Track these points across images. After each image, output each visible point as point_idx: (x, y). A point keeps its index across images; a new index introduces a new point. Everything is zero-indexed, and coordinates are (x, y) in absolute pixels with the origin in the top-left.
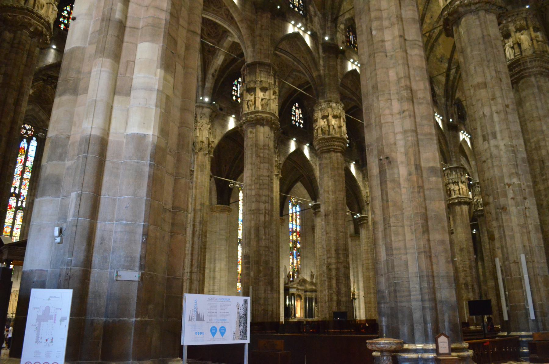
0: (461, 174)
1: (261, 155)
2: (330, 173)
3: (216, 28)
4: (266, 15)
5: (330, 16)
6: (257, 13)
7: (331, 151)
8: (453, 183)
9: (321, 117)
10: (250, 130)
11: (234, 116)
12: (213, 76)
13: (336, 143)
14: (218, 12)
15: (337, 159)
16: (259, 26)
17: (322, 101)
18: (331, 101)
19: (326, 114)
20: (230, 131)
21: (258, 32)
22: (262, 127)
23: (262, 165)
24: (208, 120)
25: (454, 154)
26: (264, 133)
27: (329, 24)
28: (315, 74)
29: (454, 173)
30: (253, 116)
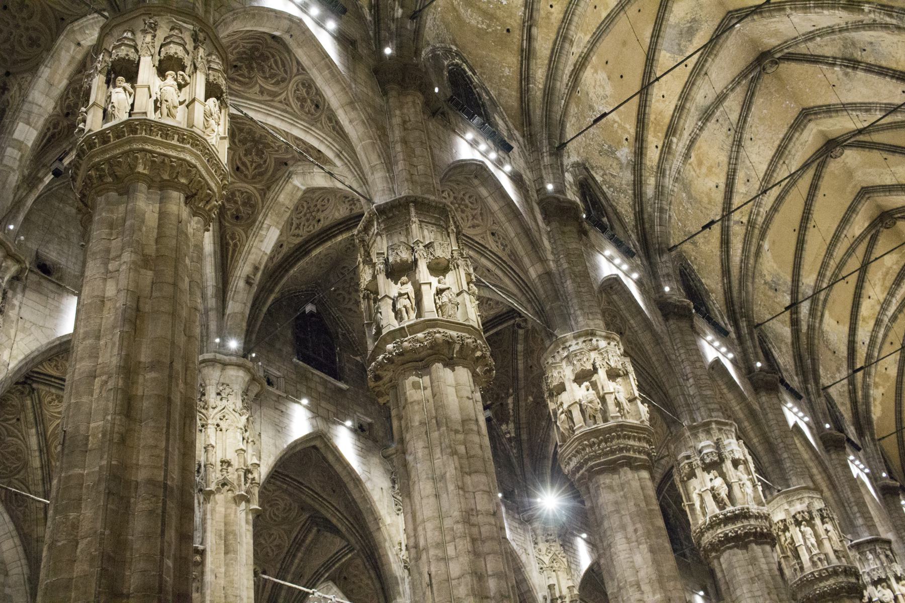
0: (887, 556)
1: (462, 449)
2: (630, 529)
3: (260, 153)
4: (410, 99)
5: (545, 142)
6: (385, 93)
7: (622, 465)
8: (875, 583)
9: (573, 377)
10: (413, 378)
11: (305, 401)
12: (248, 282)
13: (631, 442)
14: (274, 95)
15: (642, 488)
16: (396, 121)
17: (569, 335)
18: (593, 334)
19: (589, 367)
20: (296, 444)
21: (396, 134)
22: (448, 370)
23: (468, 479)
24: (239, 404)
25: (855, 509)
26: (457, 386)
27: (547, 160)
28: (533, 272)
29: (870, 556)
30: (420, 335)
